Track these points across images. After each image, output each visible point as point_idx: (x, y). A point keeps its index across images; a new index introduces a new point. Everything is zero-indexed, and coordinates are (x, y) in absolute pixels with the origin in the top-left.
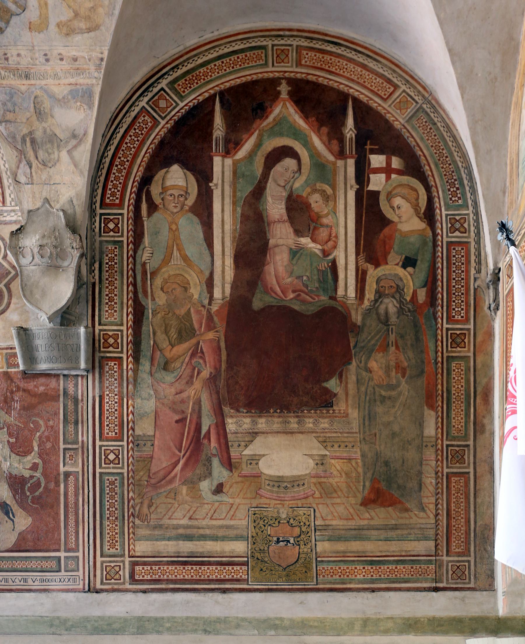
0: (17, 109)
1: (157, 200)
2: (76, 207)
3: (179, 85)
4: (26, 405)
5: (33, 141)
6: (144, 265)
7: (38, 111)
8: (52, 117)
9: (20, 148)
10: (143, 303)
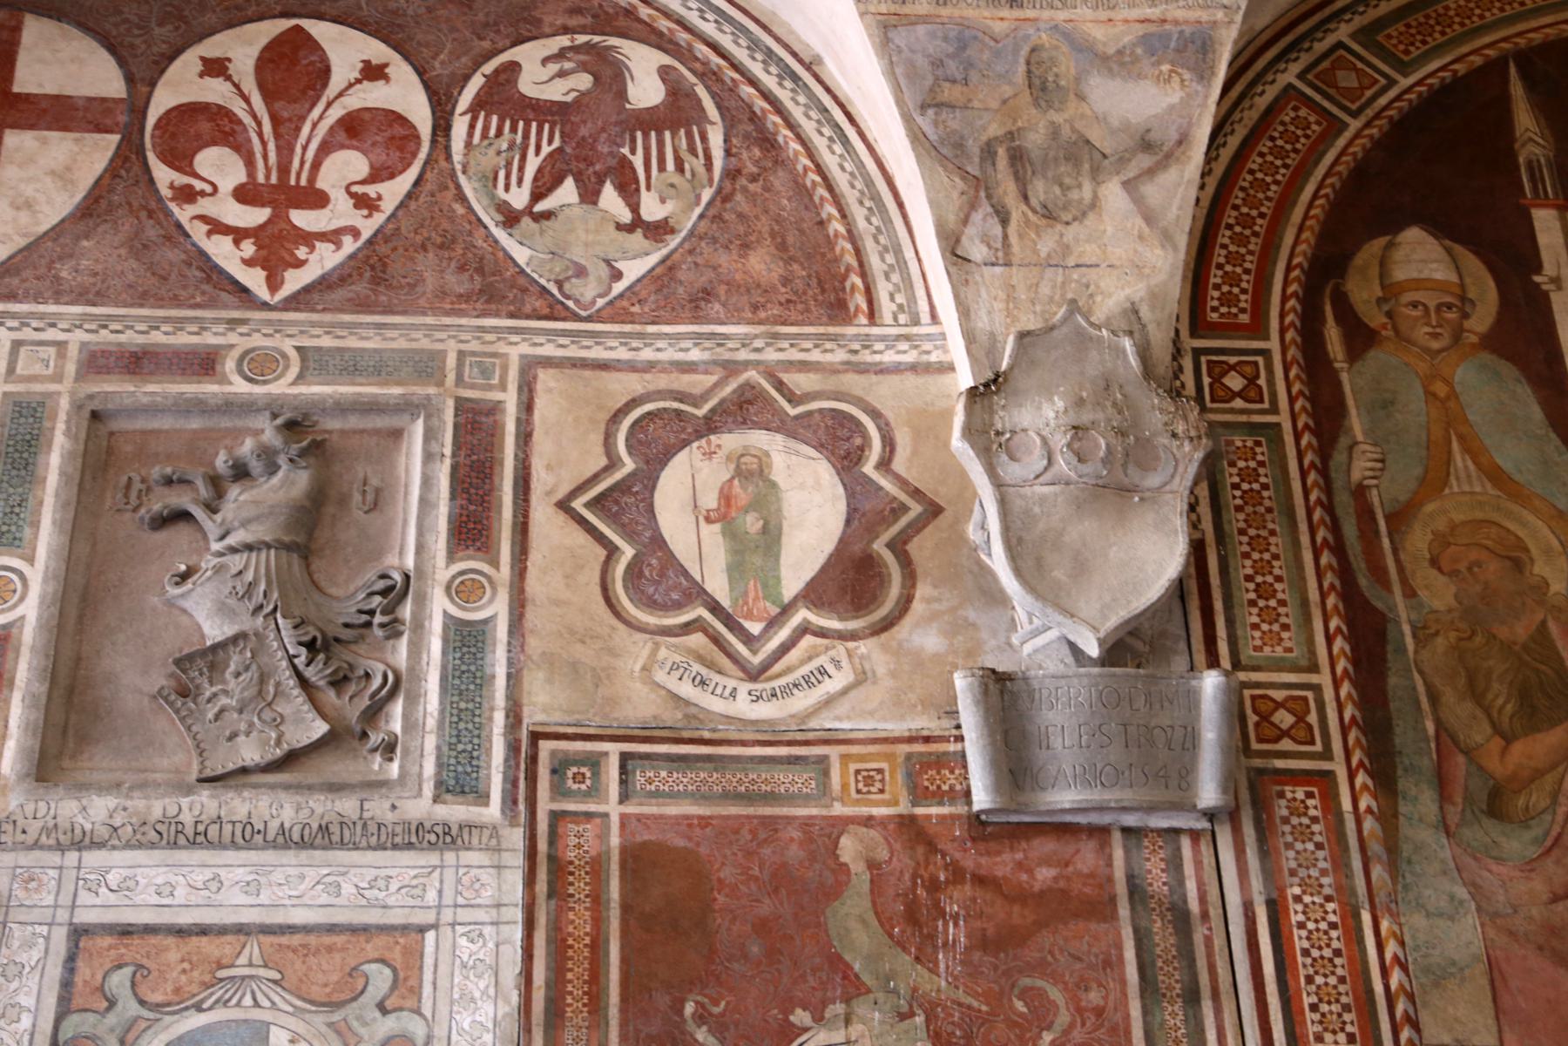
0: (974, 77)
1: (1375, 318)
2: (1151, 328)
3: (1389, 37)
4: (991, 932)
5: (1018, 158)
6: (1360, 492)
7: (1037, 82)
8: (1081, 98)
9: (977, 173)
10: (1379, 605)
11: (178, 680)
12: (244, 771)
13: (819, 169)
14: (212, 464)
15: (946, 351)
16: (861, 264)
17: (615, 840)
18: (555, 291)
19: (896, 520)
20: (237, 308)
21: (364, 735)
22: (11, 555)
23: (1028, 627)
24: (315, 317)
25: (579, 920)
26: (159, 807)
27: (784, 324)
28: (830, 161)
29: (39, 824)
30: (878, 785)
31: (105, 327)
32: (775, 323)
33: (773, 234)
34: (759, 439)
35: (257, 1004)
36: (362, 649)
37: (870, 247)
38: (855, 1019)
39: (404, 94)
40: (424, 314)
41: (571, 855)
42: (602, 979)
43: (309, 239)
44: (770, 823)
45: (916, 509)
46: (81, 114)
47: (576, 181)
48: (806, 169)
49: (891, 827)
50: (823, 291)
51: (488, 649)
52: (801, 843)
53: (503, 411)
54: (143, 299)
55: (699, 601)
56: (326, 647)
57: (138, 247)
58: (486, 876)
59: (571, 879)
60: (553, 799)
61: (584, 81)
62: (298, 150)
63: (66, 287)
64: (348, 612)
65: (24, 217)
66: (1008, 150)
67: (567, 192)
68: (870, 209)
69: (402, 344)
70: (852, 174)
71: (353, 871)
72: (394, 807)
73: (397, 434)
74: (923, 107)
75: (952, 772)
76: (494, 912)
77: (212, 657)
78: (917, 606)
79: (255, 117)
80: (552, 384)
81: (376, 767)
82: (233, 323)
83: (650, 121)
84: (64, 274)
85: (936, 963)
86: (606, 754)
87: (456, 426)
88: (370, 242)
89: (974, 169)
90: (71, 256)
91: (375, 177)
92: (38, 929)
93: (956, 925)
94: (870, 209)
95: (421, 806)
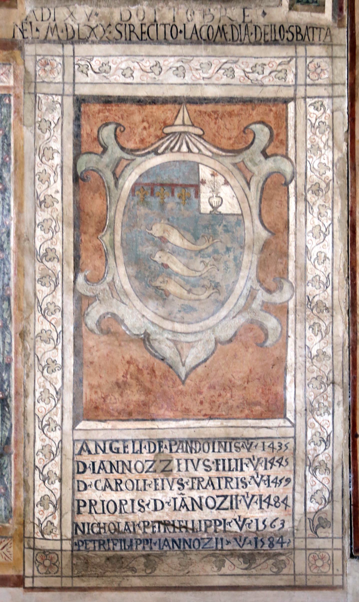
35: (190, 151)
58: (324, 64)
71: (241, 60)
72: (264, 13)
76: (330, 89)
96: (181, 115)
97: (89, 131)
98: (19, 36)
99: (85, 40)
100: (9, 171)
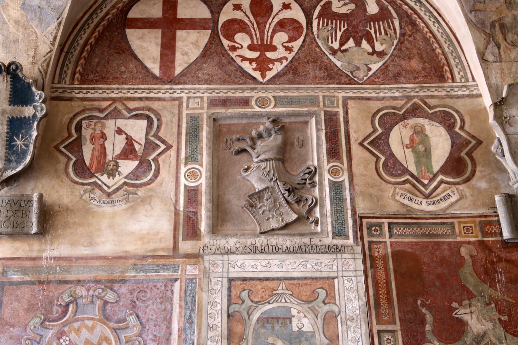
5: (502, 27)
9: (489, 32)
11: (249, 202)
12: (273, 230)
13: (431, 32)
14: (251, 134)
15: (479, 90)
16: (448, 63)
17: (389, 250)
18: (351, 75)
19: (467, 146)
20: (253, 84)
21: (308, 218)
22: (195, 164)
23: (515, 180)
24: (277, 86)
25: (381, 275)
26: (249, 241)
27: (425, 83)
28: (434, 29)
29: (214, 247)
30: (471, 231)
31: (214, 92)
32: (422, 83)
33: (418, 54)
34: (421, 121)
35: (286, 302)
36: (304, 191)
37: (450, 56)
38: (472, 305)
39: (297, 13)
40: (311, 84)
41: (376, 255)
42: (391, 293)
43: (273, 61)
44: (437, 243)
45: (474, 142)
46: (198, 24)
47: (353, 39)
48: (426, 32)
49: (477, 244)
50: (436, 72)
51: (343, 190)
52: (448, 250)
53: (339, 114)
54: (224, 82)
55: (407, 174)
56: (293, 191)
57: (221, 66)
58: (351, 262)
59: (377, 262)
60: (368, 237)
61: (352, 6)
62: (266, 33)
63: (201, 79)
64: (299, 180)
65: (185, 58)
66: (499, 24)
67: (351, 43)
68: (449, 44)
69: (305, 94)
70: (442, 33)
71: (310, 260)
72: (320, 240)
73: (306, 123)
74: (471, 12)
75: (495, 227)
76: (355, 272)
77: (259, 195)
78: (477, 173)
79: (251, 23)
80: (353, 105)
81: (313, 228)
82: (253, 89)
83: (375, 18)
84: (200, 75)
85: (496, 287)
86: (384, 223)
87: (325, 120)
88: (291, 61)
89: (488, 31)
90: (201, 70)
91: (290, 41)
92: (219, 279)
93: (501, 275)
94: (449, 44)
95: (329, 240)
96: (281, 285)
97: (235, 293)
98: (201, 252)
99: (234, 253)
100: (195, 313)
